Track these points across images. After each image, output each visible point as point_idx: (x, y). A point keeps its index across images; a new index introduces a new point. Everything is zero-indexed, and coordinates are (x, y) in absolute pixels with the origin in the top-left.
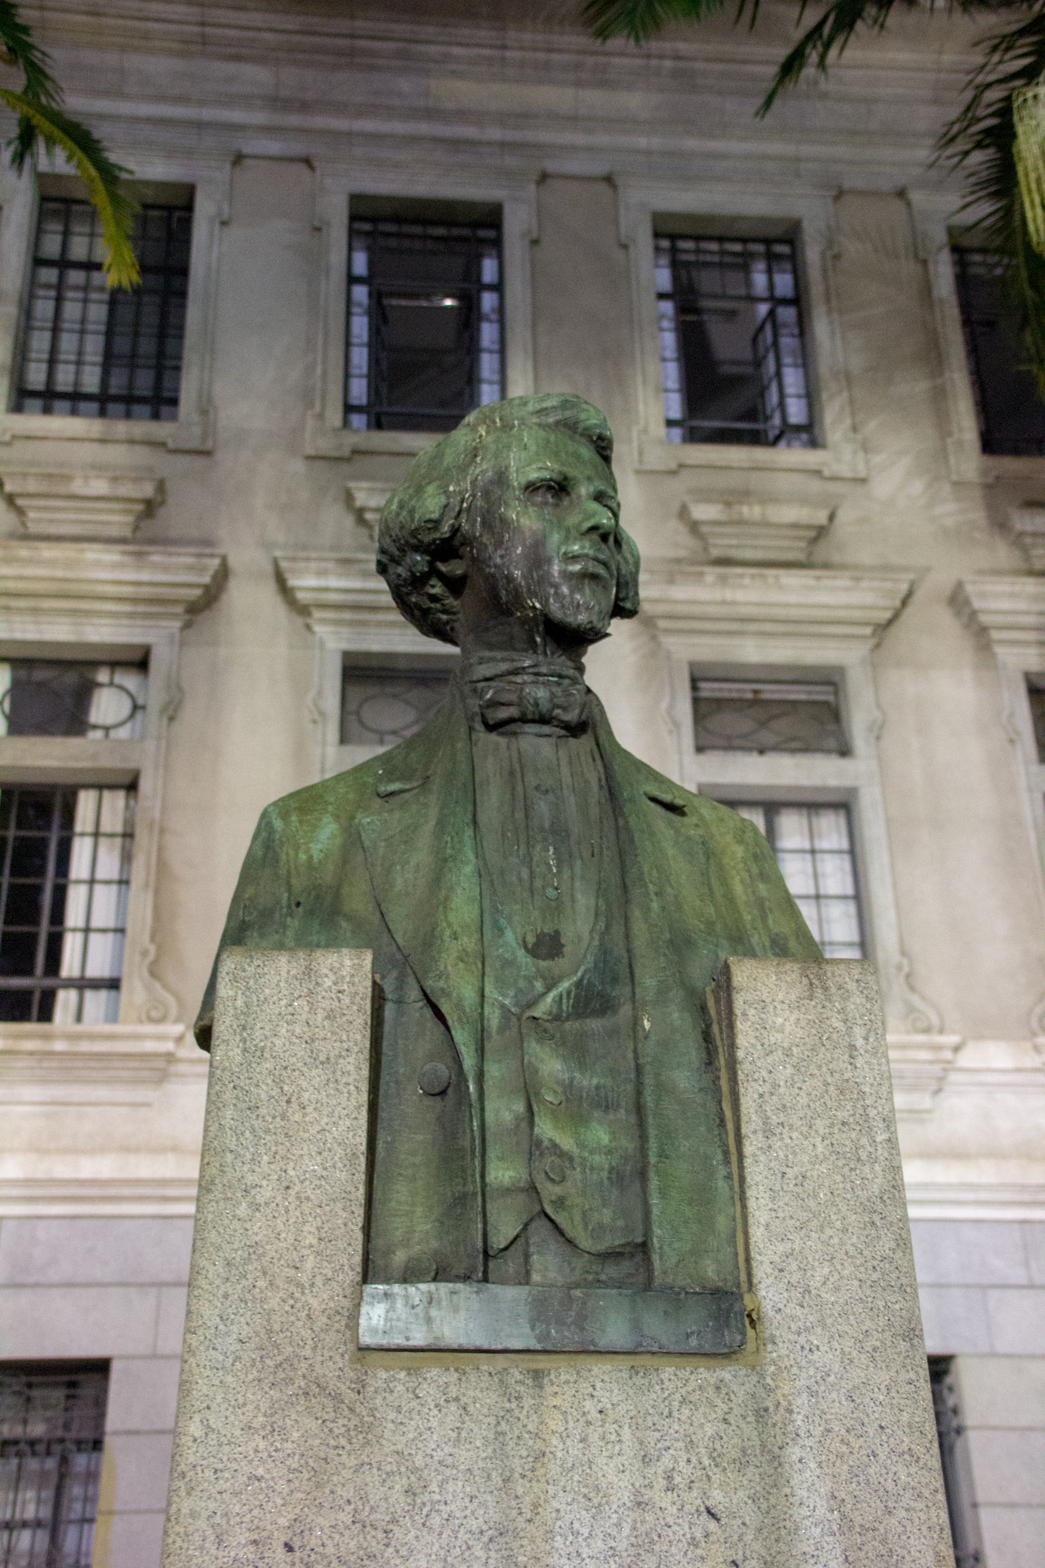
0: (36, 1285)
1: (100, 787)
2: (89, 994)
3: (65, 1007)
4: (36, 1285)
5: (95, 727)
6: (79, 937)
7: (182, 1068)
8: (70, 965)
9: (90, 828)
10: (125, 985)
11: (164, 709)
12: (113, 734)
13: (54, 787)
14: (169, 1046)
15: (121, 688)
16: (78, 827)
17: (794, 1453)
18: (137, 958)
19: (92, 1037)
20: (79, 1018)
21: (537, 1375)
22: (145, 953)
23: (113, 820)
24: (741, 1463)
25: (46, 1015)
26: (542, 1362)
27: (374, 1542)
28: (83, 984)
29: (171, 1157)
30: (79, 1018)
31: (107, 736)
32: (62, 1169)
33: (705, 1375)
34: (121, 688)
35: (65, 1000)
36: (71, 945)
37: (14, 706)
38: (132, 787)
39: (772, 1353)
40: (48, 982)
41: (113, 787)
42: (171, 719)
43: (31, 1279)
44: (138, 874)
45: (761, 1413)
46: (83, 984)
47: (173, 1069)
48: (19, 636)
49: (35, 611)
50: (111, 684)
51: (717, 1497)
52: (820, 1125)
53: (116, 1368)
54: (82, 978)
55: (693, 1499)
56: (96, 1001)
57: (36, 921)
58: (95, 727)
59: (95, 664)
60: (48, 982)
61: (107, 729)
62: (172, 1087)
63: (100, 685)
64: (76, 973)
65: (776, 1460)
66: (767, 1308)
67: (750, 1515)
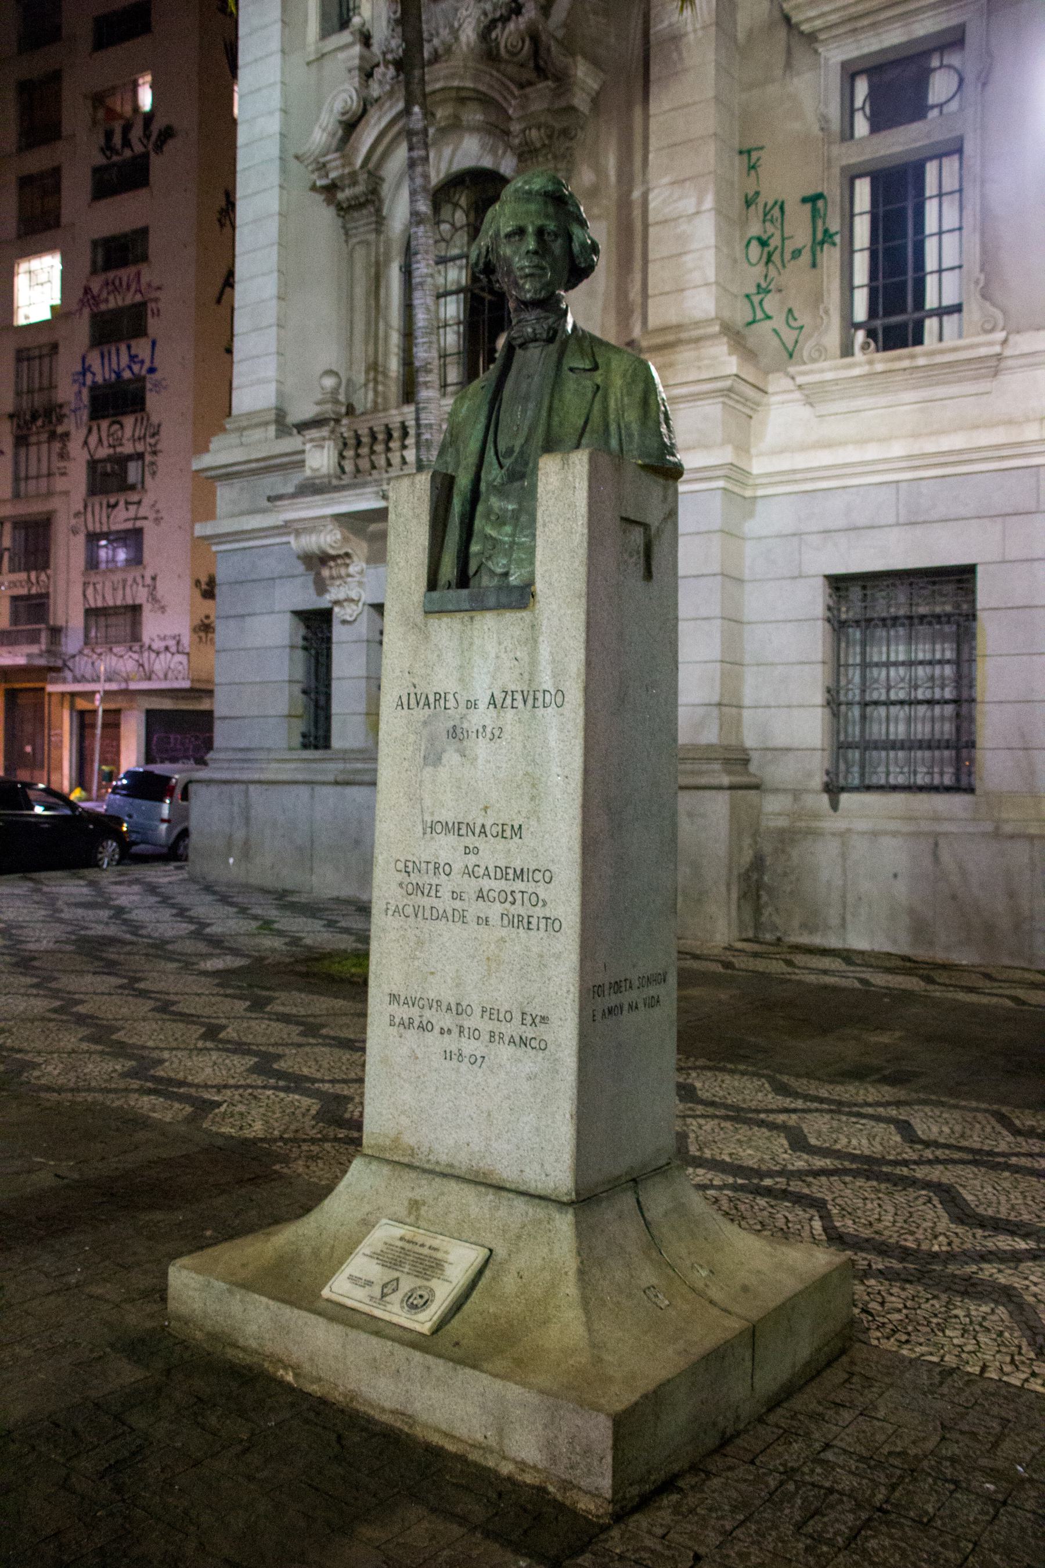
0: (924, 522)
1: (939, 157)
2: (945, 318)
3: (931, 332)
4: (924, 522)
5: (933, 107)
6: (935, 276)
7: (1010, 363)
8: (931, 301)
9: (935, 192)
10: (965, 308)
11: (978, 78)
12: (945, 109)
13: (906, 164)
14: (997, 349)
15: (949, 67)
16: (928, 193)
17: (541, 639)
18: (972, 286)
19: (955, 350)
20: (941, 339)
21: (472, 618)
22: (977, 282)
23: (950, 183)
24: (526, 644)
25: (919, 340)
26: (473, 613)
27: (429, 671)
28: (942, 312)
29: (1001, 429)
30: (941, 339)
31: (941, 112)
32: (930, 446)
33: (510, 616)
34: (949, 67)
35: (931, 325)
36: (931, 283)
37: (871, 110)
38: (959, 151)
39: (537, 606)
40: (917, 315)
41: (948, 154)
42: (984, 84)
43: (921, 519)
44: (969, 222)
45: (533, 626)
46: (942, 312)
47: (1003, 365)
48: (866, 50)
49: (873, 25)
50: (941, 67)
51: (518, 654)
52: (561, 521)
53: (980, 570)
54: (940, 307)
55: (512, 655)
56: (950, 322)
57: (905, 273)
58: (933, 107)
59: (927, 54)
60: (917, 315)
61: (941, 106)
62: (1004, 378)
63: (934, 70)
64: (935, 305)
65: (536, 641)
66: (538, 591)
67: (527, 659)
